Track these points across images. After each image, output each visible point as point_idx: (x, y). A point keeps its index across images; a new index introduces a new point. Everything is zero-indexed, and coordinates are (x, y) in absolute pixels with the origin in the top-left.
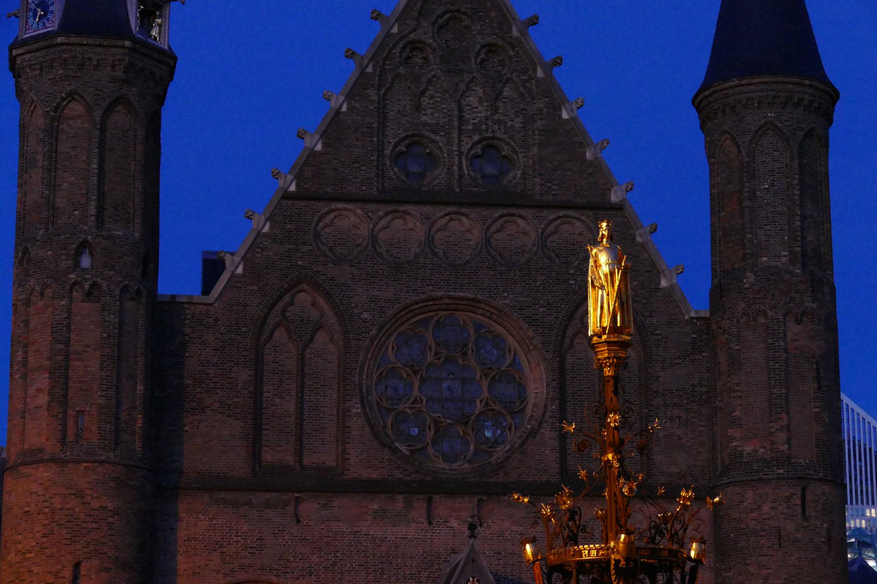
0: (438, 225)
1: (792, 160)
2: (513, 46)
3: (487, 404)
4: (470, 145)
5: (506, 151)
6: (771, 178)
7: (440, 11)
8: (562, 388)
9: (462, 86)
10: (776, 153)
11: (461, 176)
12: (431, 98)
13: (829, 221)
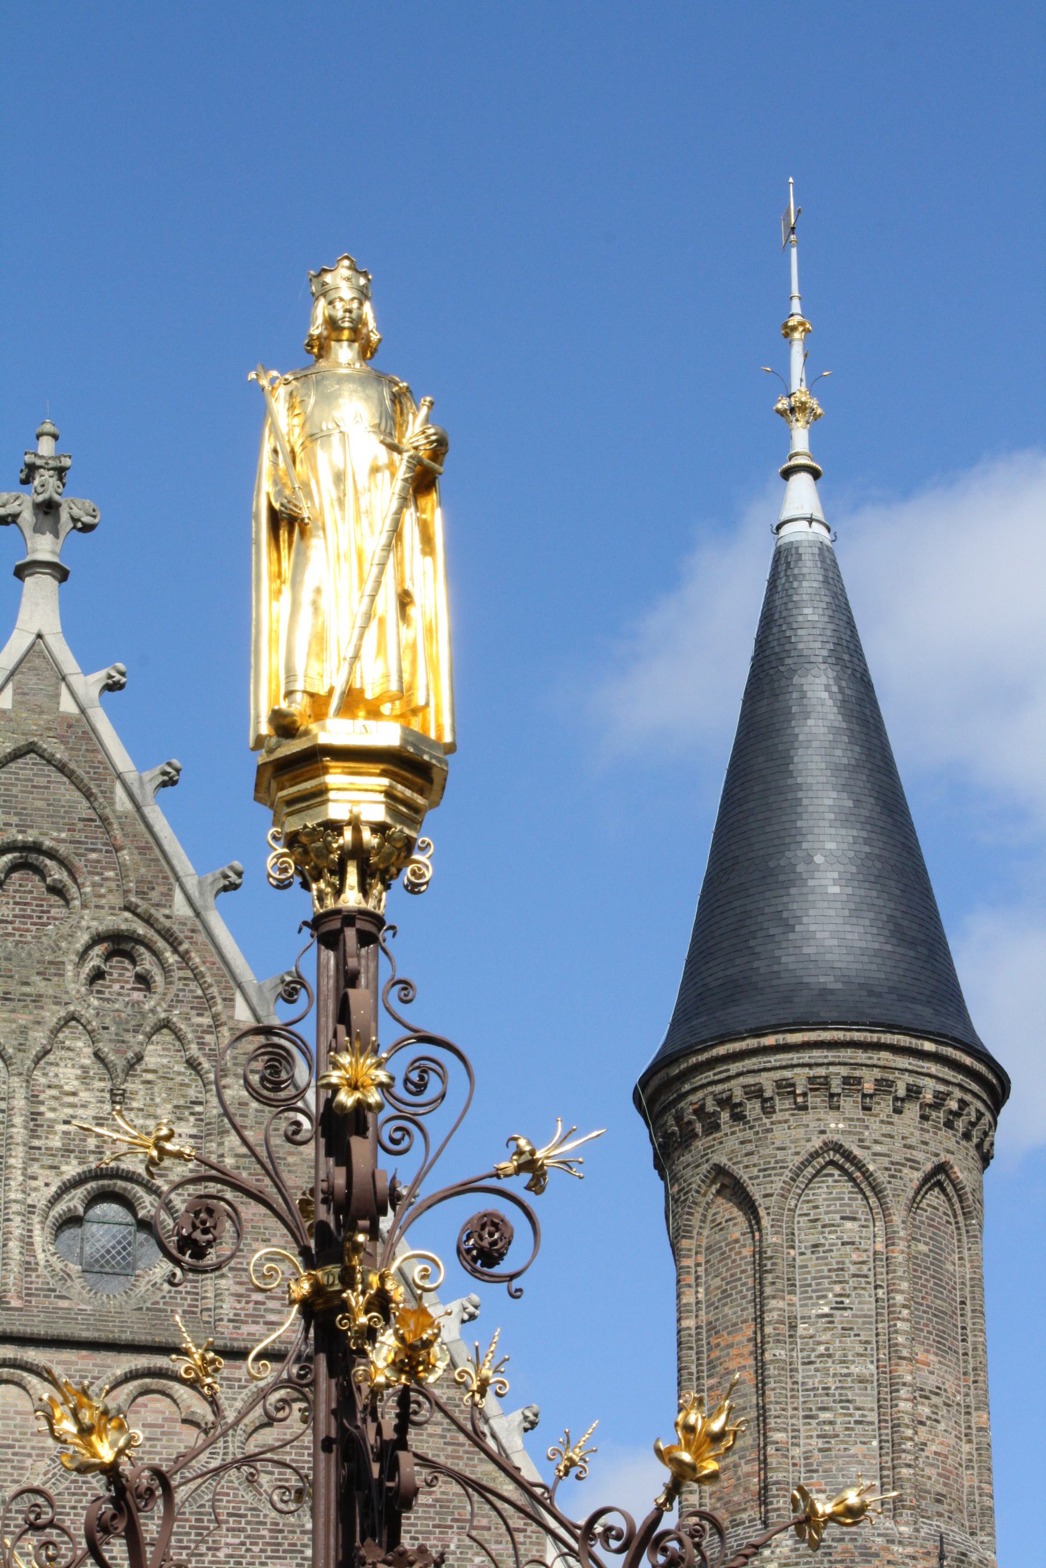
1: (890, 1242)
2: (174, 943)
4: (53, 1189)
6: (837, 1288)
9: (39, 1037)
10: (849, 1225)
11: (29, 1267)
13: (983, 1405)
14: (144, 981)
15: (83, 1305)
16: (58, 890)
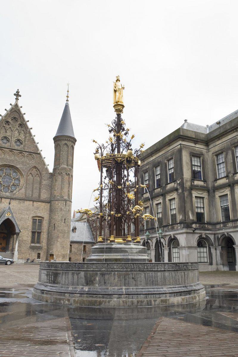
0: (8, 152)
3: (13, 183)
5: (21, 142)
7: (12, 116)
8: (26, 182)
9: (15, 130)
11: (13, 145)
12: (9, 131)
14: (22, 127)
15: (16, 147)
16: (16, 120)
